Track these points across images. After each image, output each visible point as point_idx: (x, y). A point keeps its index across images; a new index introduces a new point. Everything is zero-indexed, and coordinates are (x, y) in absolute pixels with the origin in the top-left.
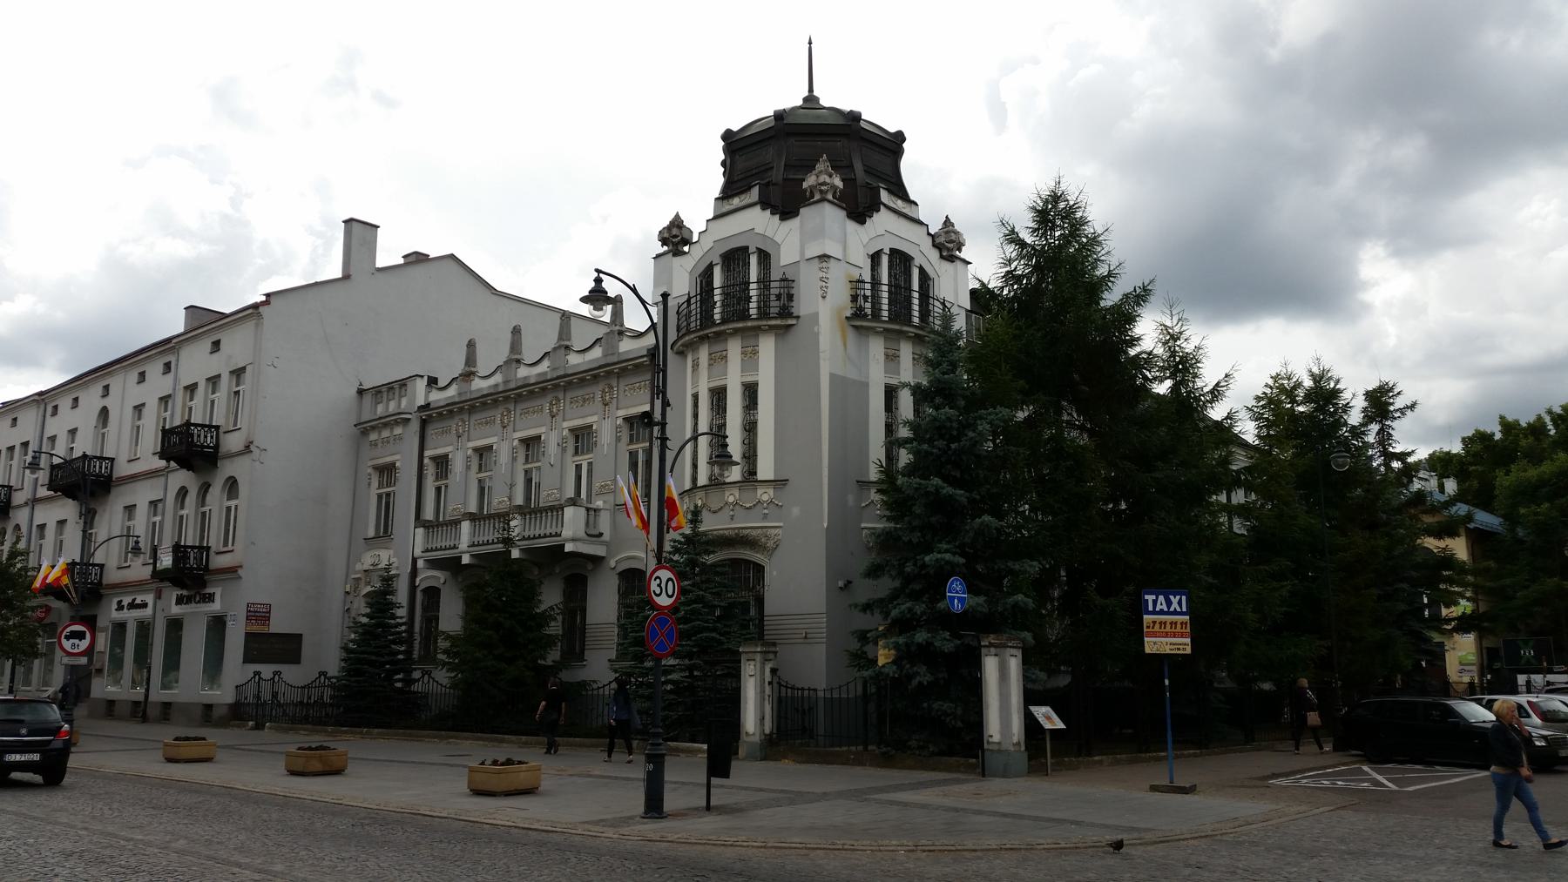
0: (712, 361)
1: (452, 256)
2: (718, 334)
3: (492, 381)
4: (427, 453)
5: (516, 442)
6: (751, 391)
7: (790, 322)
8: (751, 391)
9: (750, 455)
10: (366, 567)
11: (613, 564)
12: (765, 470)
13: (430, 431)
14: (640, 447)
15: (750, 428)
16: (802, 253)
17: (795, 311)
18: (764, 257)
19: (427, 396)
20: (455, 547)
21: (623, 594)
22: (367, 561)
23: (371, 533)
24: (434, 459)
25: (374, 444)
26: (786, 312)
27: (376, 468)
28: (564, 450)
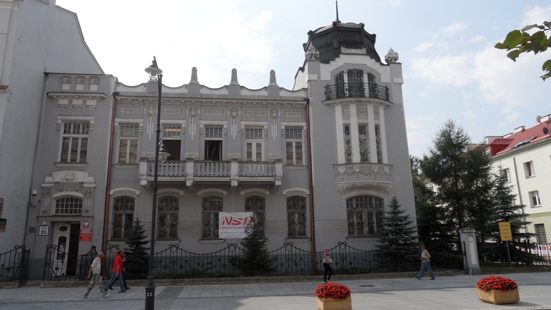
0: (359, 112)
1: (75, 15)
2: (366, 101)
3: (178, 91)
4: (117, 120)
5: (202, 126)
6: (377, 128)
7: (391, 104)
8: (377, 128)
9: (379, 154)
10: (56, 180)
11: (284, 192)
12: (385, 160)
13: (122, 110)
14: (294, 141)
15: (378, 143)
16: (392, 80)
17: (390, 100)
18: (371, 77)
19: (115, 88)
20: (228, 176)
21: (289, 207)
22: (60, 176)
23: (59, 160)
24: (120, 124)
25: (65, 107)
26: (387, 100)
27: (63, 121)
28: (242, 135)
